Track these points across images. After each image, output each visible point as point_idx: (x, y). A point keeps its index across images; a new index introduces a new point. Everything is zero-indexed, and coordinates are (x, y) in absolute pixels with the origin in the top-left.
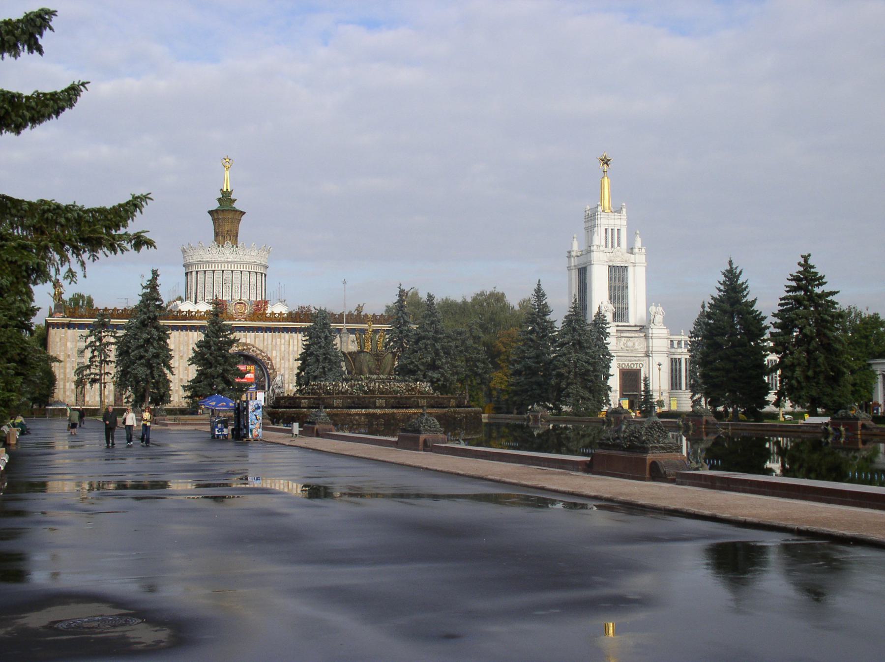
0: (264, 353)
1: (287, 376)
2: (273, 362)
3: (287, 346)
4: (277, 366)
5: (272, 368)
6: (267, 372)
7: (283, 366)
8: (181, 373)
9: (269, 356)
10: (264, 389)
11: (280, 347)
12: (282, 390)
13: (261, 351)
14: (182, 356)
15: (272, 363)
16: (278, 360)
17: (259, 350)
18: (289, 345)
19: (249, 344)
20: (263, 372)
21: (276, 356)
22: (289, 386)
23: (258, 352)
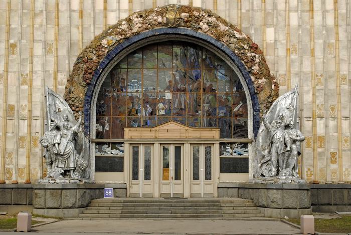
0: (239, 31)
1: (308, 98)
2: (267, 58)
3: (306, 16)
4: (279, 69)
5: (265, 72)
6: (250, 83)
7: (295, 69)
8: (12, 89)
9: (255, 40)
10: (245, 135)
11: (287, 19)
12: (294, 133)
13: (231, 26)
14: (13, 46)
15: (263, 60)
16: (282, 52)
17: (225, 23)
18: (312, 10)
19: (198, 10)
20: (239, 87)
21: (276, 41)
22: (314, 125)
23: (222, 27)
